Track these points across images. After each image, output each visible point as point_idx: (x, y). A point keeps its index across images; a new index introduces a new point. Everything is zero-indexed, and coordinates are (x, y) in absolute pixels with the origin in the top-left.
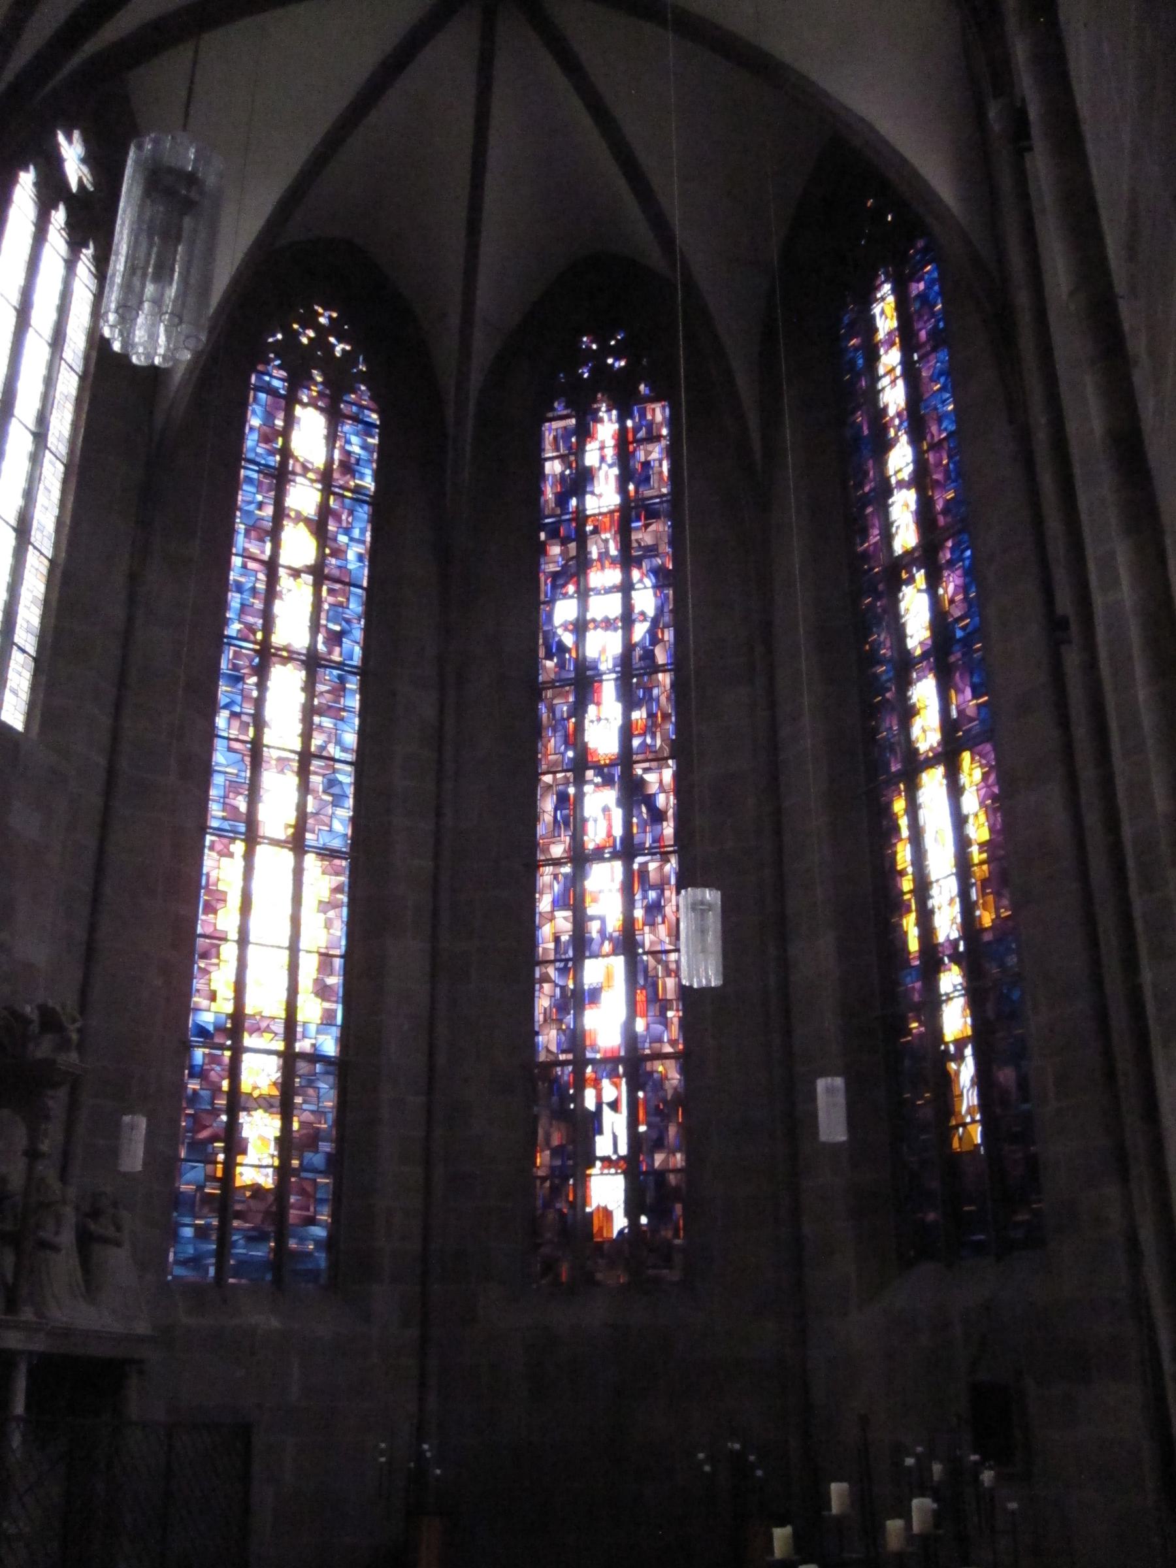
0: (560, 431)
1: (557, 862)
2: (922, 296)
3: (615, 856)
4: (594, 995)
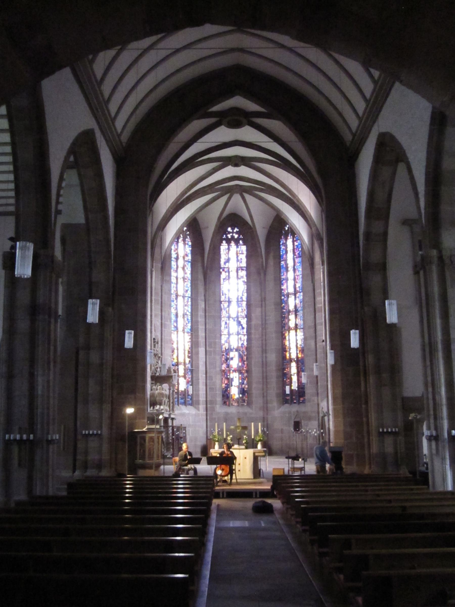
0: (224, 248)
1: (225, 335)
2: (296, 245)
3: (236, 334)
4: (232, 359)
